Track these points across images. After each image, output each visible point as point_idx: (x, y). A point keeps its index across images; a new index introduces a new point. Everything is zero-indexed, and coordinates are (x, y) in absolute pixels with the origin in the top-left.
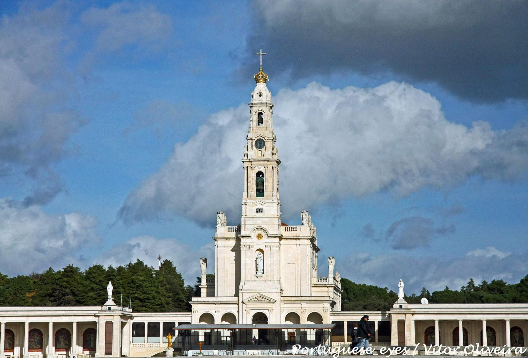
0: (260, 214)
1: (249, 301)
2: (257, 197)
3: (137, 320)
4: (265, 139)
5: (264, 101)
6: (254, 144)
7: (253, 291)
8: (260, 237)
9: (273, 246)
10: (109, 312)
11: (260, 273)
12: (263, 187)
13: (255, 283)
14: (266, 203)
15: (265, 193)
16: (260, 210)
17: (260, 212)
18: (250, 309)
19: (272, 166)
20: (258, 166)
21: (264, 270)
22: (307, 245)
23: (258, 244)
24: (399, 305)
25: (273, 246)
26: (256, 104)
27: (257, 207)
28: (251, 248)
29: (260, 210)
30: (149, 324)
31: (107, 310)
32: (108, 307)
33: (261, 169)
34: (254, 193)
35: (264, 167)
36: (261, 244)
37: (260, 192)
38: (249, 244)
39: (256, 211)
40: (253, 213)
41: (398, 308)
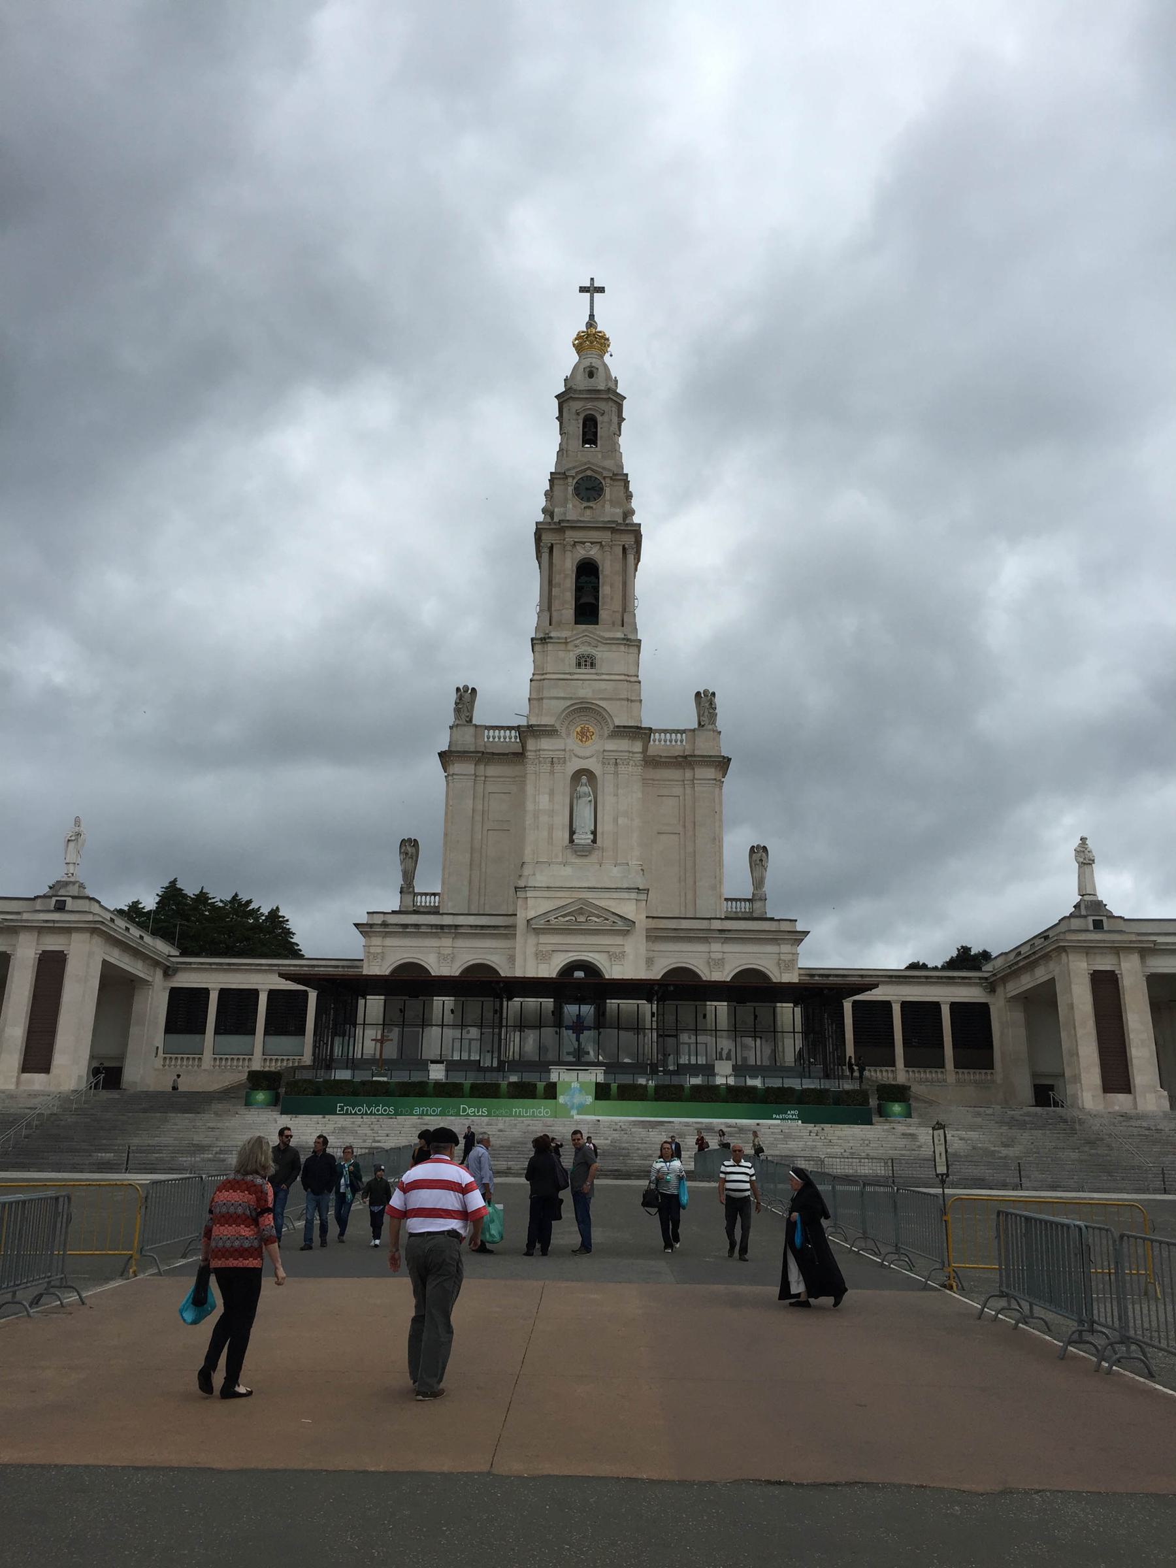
0: (585, 673)
1: (548, 921)
2: (575, 624)
3: (187, 980)
4: (604, 478)
5: (602, 387)
6: (570, 489)
8: (584, 735)
10: (56, 916)
11: (583, 838)
12: (597, 599)
13: (568, 871)
15: (603, 614)
16: (586, 661)
17: (586, 665)
18: (550, 948)
19: (624, 546)
20: (585, 543)
21: (594, 833)
22: (714, 782)
24: (1090, 919)
27: (578, 651)
28: (557, 768)
29: (586, 661)
30: (223, 992)
31: (52, 911)
32: (57, 901)
33: (592, 553)
34: (569, 613)
35: (601, 545)
36: (588, 754)
37: (587, 612)
38: (551, 753)
39: (574, 662)
41: (1087, 931)
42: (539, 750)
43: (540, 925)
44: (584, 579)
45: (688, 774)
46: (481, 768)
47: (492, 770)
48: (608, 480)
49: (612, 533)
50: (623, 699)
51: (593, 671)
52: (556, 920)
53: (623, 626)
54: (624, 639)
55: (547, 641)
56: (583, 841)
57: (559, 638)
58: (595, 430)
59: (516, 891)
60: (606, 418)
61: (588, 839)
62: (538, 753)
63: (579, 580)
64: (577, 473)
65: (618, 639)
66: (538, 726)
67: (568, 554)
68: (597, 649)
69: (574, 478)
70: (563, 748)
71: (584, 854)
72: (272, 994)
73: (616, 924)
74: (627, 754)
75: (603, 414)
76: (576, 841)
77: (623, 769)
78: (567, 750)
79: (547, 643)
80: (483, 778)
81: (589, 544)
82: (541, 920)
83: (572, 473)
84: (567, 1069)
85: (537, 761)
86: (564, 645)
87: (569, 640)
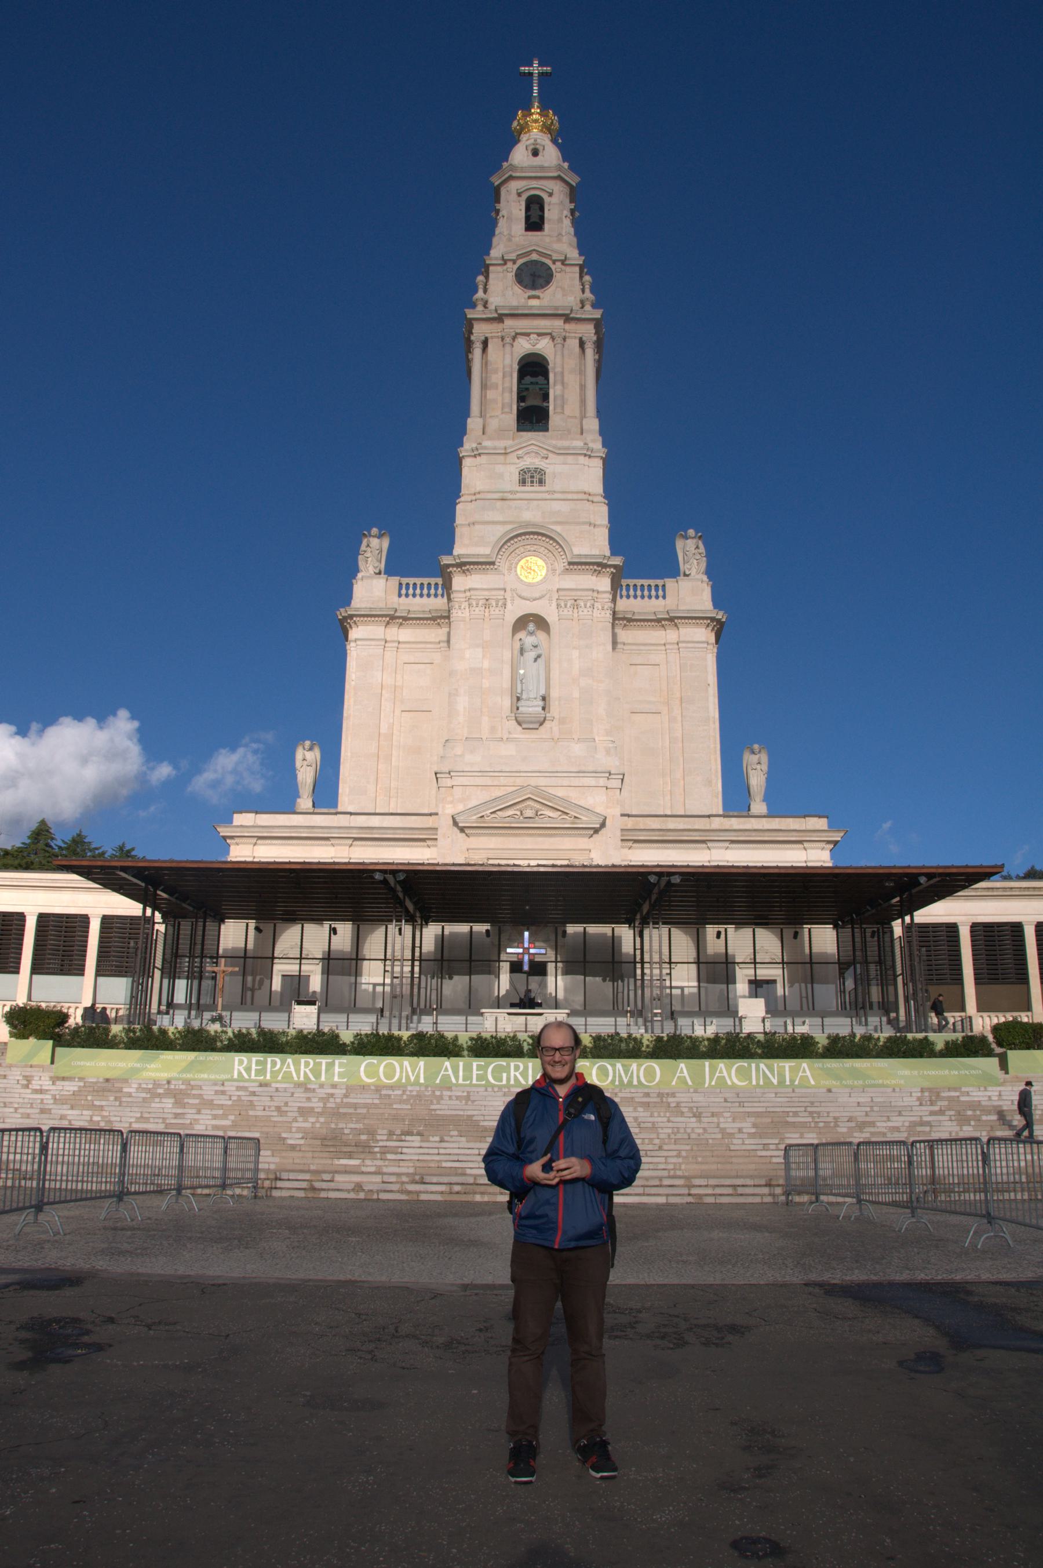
1: (483, 816)
6: (511, 276)
7: (503, 781)
9: (588, 604)
11: (531, 708)
14: (560, 449)
15: (554, 419)
17: (532, 482)
20: (528, 335)
23: (524, 594)
25: (588, 604)
26: (522, 169)
29: (532, 477)
30: (43, 919)
33: (539, 346)
34: (511, 418)
35: (553, 339)
36: (537, 595)
38: (486, 593)
39: (516, 477)
40: (508, 487)
42: (470, 590)
43: (472, 820)
44: (528, 379)
45: (671, 635)
46: (395, 633)
47: (406, 634)
48: (559, 264)
49: (564, 323)
50: (584, 523)
51: (542, 489)
52: (493, 816)
53: (582, 433)
54: (582, 449)
55: (480, 451)
56: (530, 709)
57: (495, 448)
58: (541, 214)
59: (437, 778)
60: (554, 200)
61: (538, 706)
62: (468, 594)
63: (523, 382)
64: (519, 256)
65: (574, 448)
66: (468, 556)
67: (508, 348)
68: (547, 461)
69: (514, 262)
70: (502, 586)
71: (531, 726)
72: (107, 921)
73: (577, 821)
74: (590, 593)
75: (551, 195)
76: (520, 709)
77: (586, 612)
78: (508, 589)
79: (480, 455)
80: (396, 644)
81: (535, 336)
82: (472, 816)
83: (513, 256)
84: (509, 1014)
85: (465, 605)
86: (502, 457)
87: (508, 451)
